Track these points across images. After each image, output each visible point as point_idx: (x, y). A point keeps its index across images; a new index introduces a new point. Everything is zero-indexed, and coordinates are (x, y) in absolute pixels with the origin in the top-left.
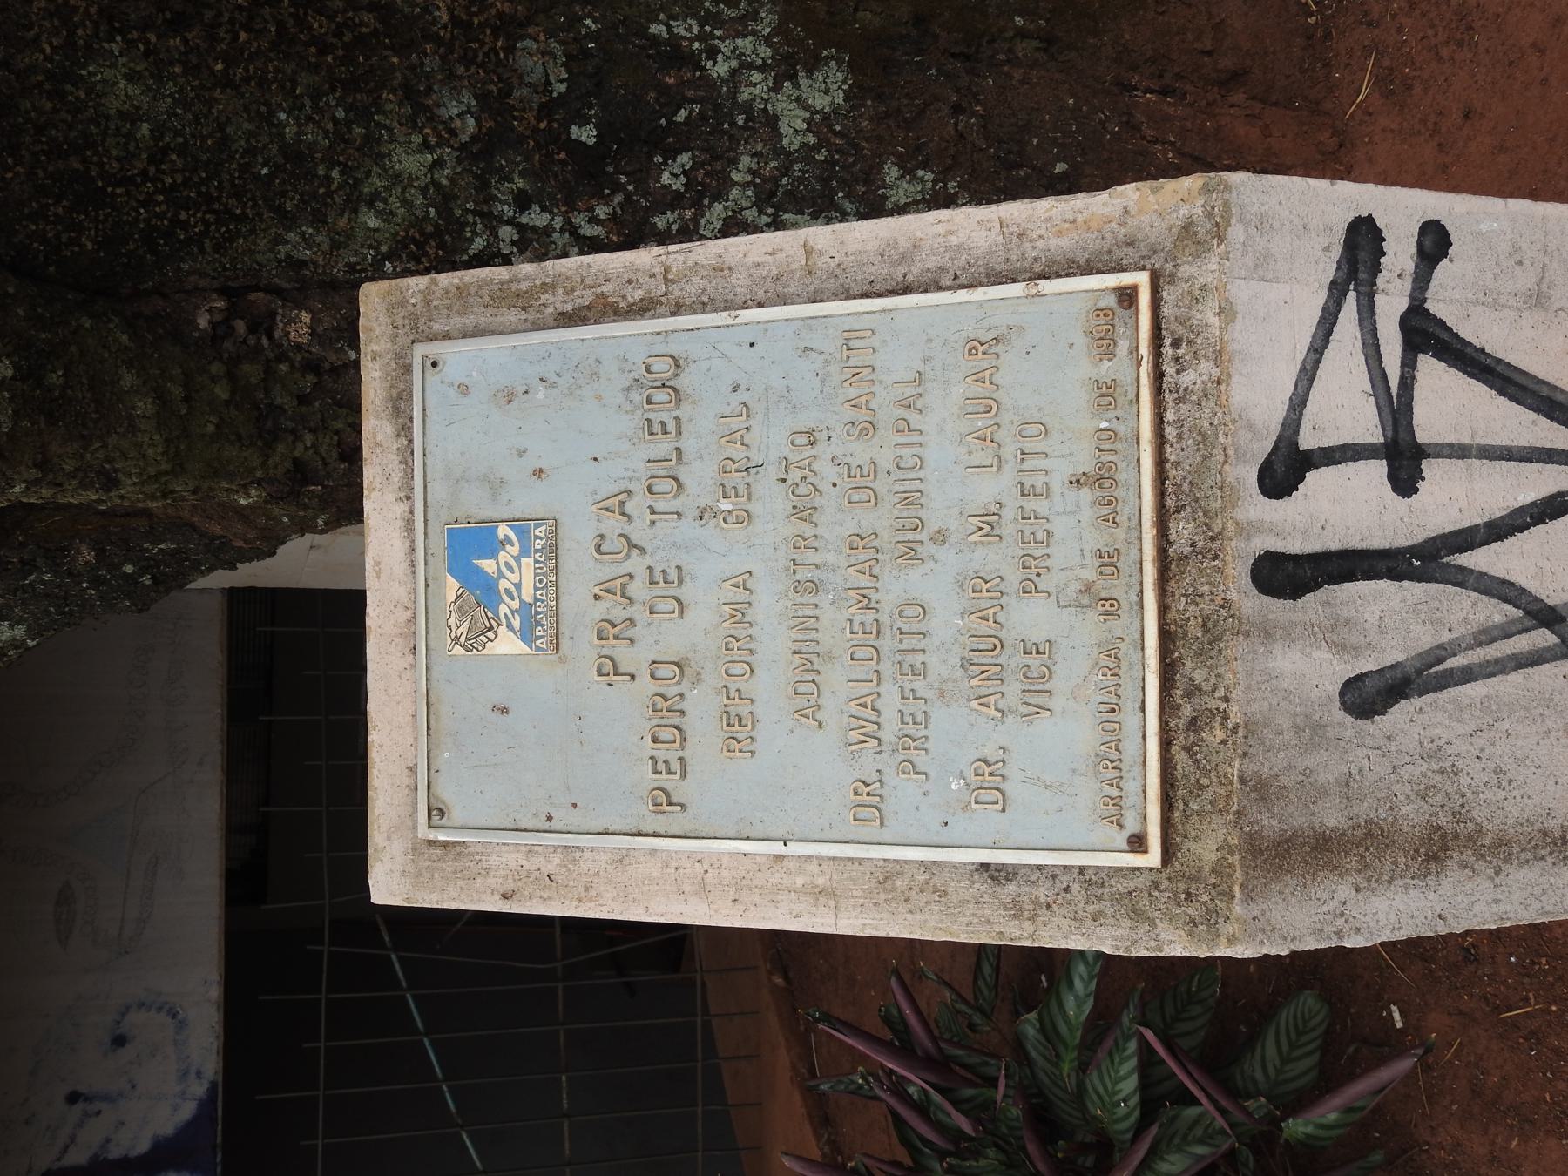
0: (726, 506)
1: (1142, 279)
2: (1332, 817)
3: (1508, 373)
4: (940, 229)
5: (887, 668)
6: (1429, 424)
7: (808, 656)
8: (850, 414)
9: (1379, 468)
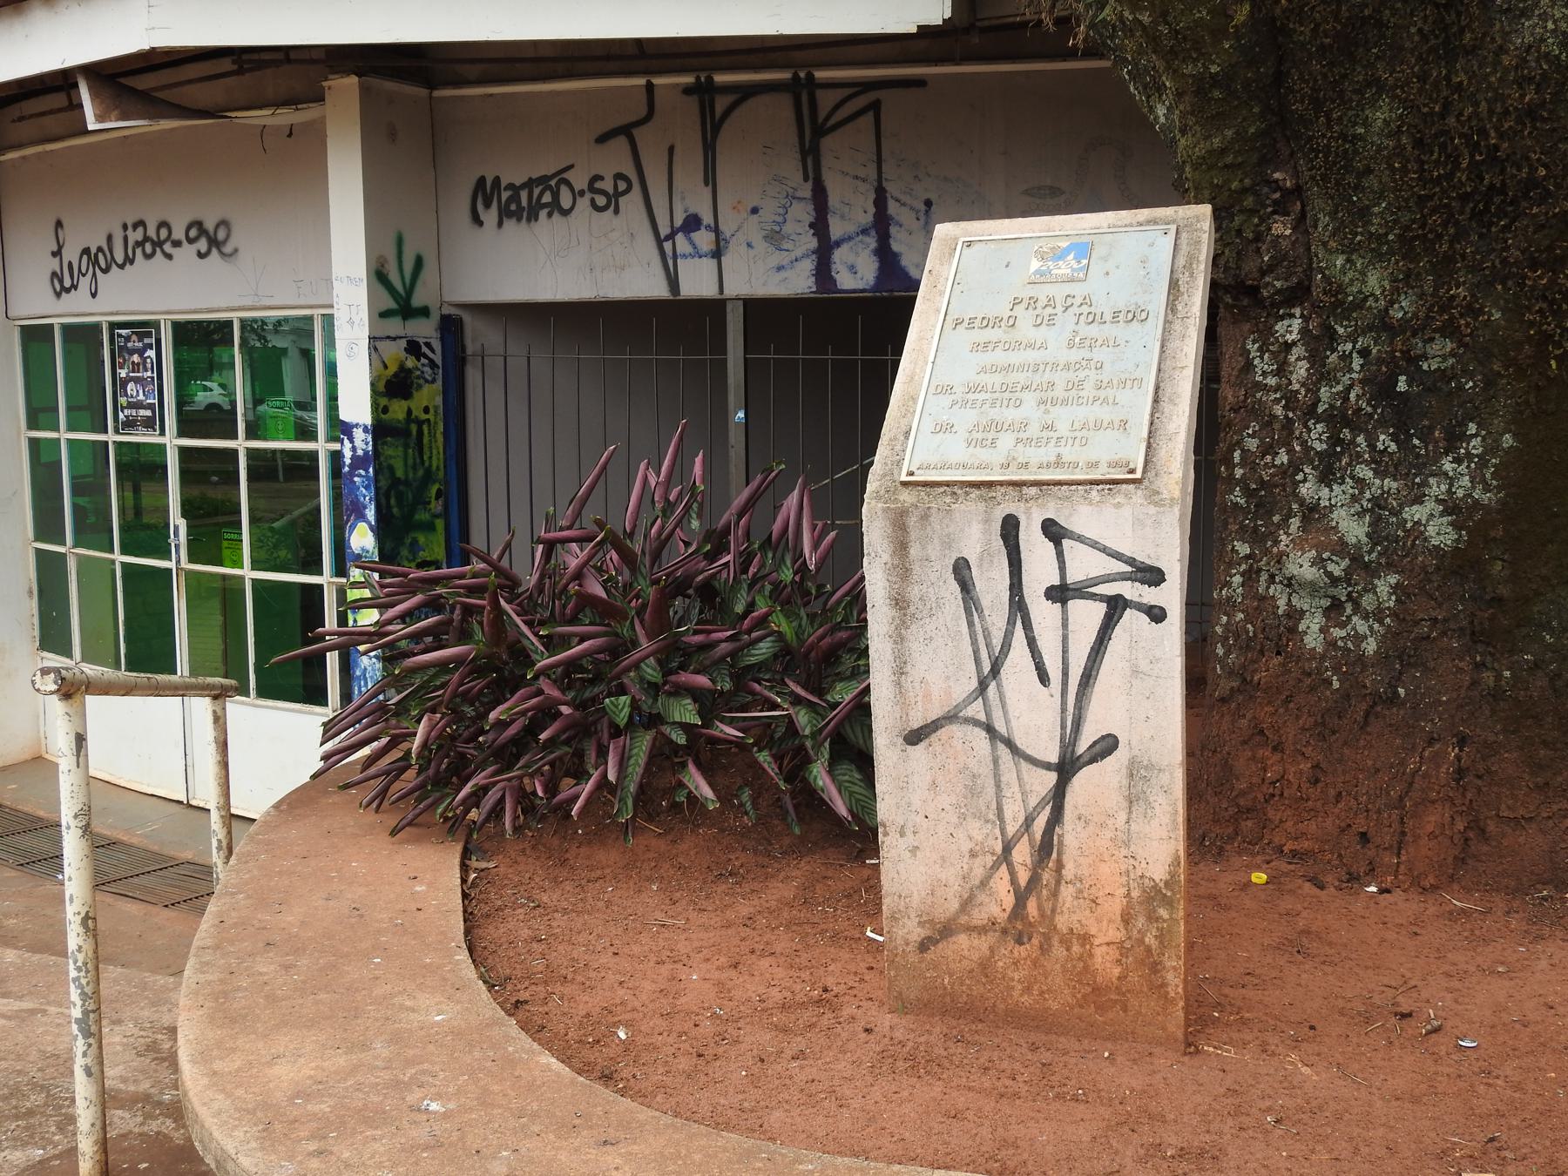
0: (1077, 340)
1: (1138, 475)
2: (914, 551)
3: (1101, 652)
4: (1181, 412)
5: (997, 395)
6: (1075, 605)
7: (1008, 368)
8: (1105, 381)
9: (1057, 582)
